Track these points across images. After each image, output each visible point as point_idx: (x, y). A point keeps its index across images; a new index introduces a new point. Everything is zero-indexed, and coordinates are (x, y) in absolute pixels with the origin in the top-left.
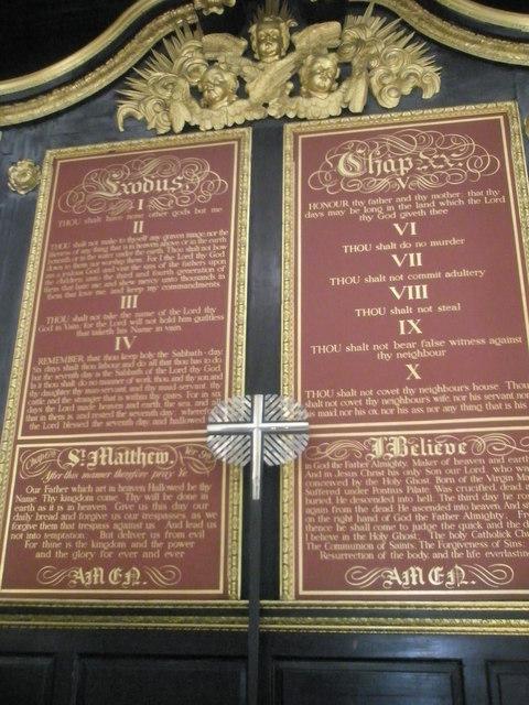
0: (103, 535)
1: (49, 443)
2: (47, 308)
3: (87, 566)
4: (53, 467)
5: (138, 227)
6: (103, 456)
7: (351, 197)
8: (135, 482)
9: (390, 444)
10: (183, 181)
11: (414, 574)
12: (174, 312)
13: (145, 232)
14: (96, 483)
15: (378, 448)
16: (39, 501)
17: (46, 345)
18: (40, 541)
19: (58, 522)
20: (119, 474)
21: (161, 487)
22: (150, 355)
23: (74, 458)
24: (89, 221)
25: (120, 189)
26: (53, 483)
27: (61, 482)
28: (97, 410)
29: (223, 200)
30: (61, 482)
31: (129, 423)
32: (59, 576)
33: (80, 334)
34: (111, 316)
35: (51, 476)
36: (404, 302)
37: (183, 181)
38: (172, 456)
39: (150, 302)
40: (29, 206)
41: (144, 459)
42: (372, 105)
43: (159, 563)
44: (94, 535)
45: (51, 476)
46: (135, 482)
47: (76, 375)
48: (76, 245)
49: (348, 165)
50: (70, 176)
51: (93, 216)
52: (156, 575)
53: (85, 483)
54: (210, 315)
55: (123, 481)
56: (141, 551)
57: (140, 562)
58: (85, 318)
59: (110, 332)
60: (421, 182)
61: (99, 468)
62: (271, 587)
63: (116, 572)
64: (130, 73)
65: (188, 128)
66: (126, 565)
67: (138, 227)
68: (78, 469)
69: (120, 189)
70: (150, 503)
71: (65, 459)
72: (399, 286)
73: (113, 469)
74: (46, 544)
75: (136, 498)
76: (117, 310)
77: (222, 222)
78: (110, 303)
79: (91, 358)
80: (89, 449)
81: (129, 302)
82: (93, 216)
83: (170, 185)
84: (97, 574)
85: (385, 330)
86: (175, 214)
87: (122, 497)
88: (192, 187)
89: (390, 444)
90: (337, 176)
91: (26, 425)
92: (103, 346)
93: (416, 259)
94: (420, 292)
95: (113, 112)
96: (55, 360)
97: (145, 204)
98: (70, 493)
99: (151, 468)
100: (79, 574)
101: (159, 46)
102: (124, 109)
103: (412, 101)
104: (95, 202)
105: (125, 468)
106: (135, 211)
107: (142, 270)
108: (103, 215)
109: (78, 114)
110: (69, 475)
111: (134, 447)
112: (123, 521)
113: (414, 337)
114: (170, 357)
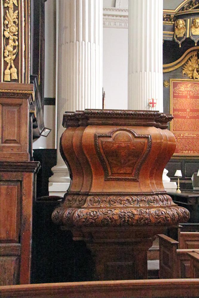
0: (187, 146)
1: (178, 133)
3: (185, 151)
4: (179, 136)
6: (186, 135)
8: (191, 139)
10: (195, 89)
12: (195, 113)
13: (190, 98)
14: (186, 139)
18: (178, 147)
19: (181, 144)
20: (189, 138)
21: (195, 140)
22: (192, 120)
23: (182, 135)
24: (180, 95)
25: (185, 89)
26: (179, 139)
27: (180, 139)
28: (185, 128)
30: (180, 139)
31: (190, 130)
32: (181, 152)
33: (180, 115)
34: (185, 113)
35: (178, 137)
37: (195, 89)
38: (196, 135)
41: (192, 136)
43: (196, 150)
44: (186, 146)
45: (178, 137)
46: (191, 139)
47: (180, 122)
48: (178, 99)
51: (181, 94)
52: (195, 152)
53: (184, 139)
55: (190, 139)
56: (193, 149)
57: (193, 150)
58: (181, 112)
59: (185, 115)
61: (186, 137)
63: (189, 151)
64: (184, 64)
66: (191, 150)
67: (188, 97)
68: (182, 137)
69: (185, 89)
70: (194, 142)
71: (180, 135)
73: (188, 137)
74: (179, 147)
75: (192, 141)
76: (187, 112)
79: (183, 119)
80: (184, 134)
82: (181, 94)
83: (193, 89)
84: (187, 152)
86: (194, 95)
87: (190, 141)
88: (197, 90)
91: (173, 129)
92: (185, 117)
95: (182, 72)
96: (177, 119)
97: (189, 92)
98: (182, 140)
100: (184, 152)
101: (189, 59)
102: (184, 72)
104: (180, 91)
105: (190, 137)
106: (188, 94)
107: (190, 105)
108: (182, 94)
109: (175, 71)
110: (181, 138)
111: (191, 134)
112: (190, 144)
114: (195, 120)
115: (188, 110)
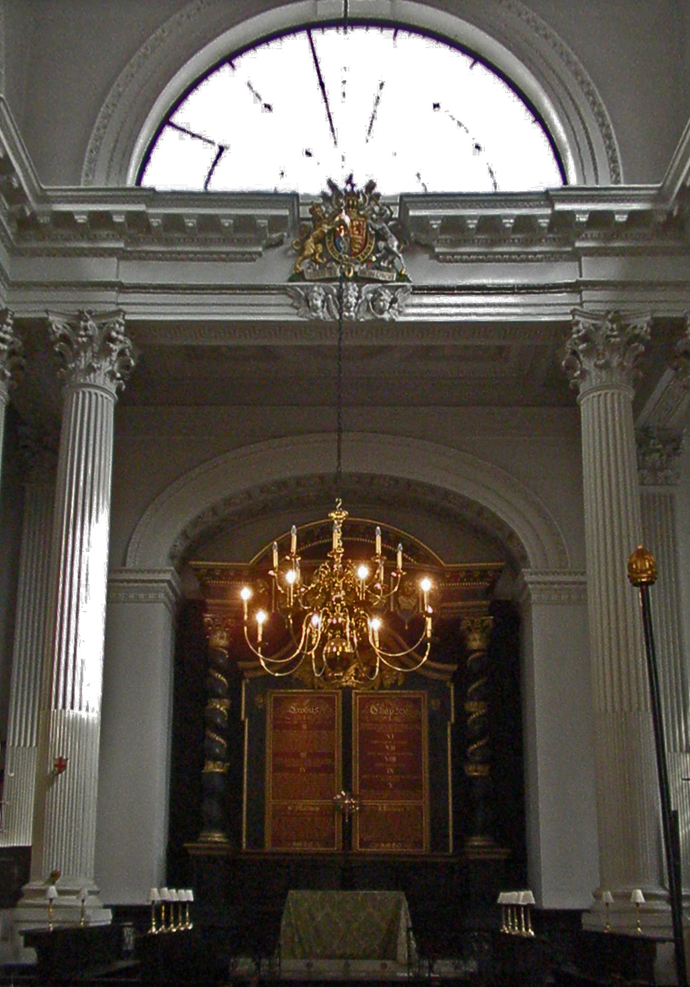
2: (275, 755)
3: (297, 841)
5: (304, 727)
6: (299, 807)
7: (374, 722)
9: (383, 806)
11: (388, 845)
15: (380, 809)
16: (280, 821)
17: (277, 768)
29: (333, 719)
36: (389, 762)
39: (309, 755)
40: (264, 711)
42: (381, 687)
49: (373, 709)
50: (278, 702)
54: (328, 761)
60: (396, 719)
62: (350, 848)
65: (319, 688)
66: (309, 841)
67: (304, 727)
72: (388, 757)
77: (331, 727)
78: (296, 755)
81: (303, 755)
84: (300, 844)
85: (383, 771)
89: (383, 806)
90: (370, 713)
92: (297, 770)
93: (393, 748)
94: (394, 759)
99: (314, 812)
100: (294, 844)
103: (394, 686)
104: (288, 714)
113: (391, 774)
115: (303, 755)
